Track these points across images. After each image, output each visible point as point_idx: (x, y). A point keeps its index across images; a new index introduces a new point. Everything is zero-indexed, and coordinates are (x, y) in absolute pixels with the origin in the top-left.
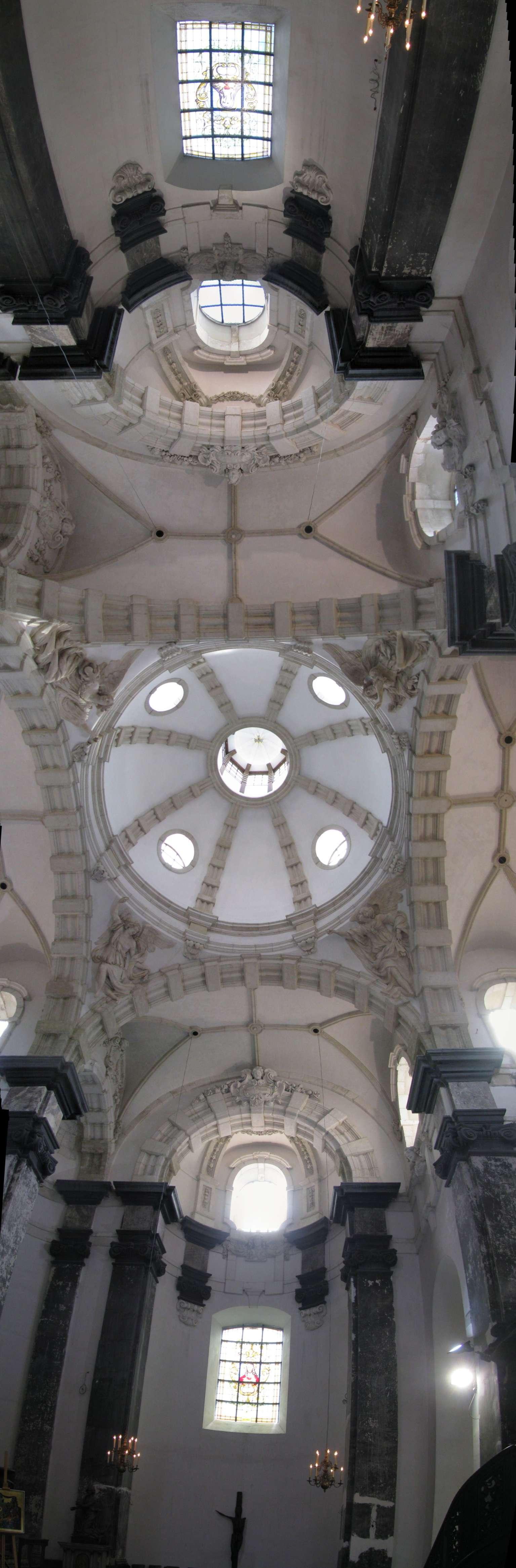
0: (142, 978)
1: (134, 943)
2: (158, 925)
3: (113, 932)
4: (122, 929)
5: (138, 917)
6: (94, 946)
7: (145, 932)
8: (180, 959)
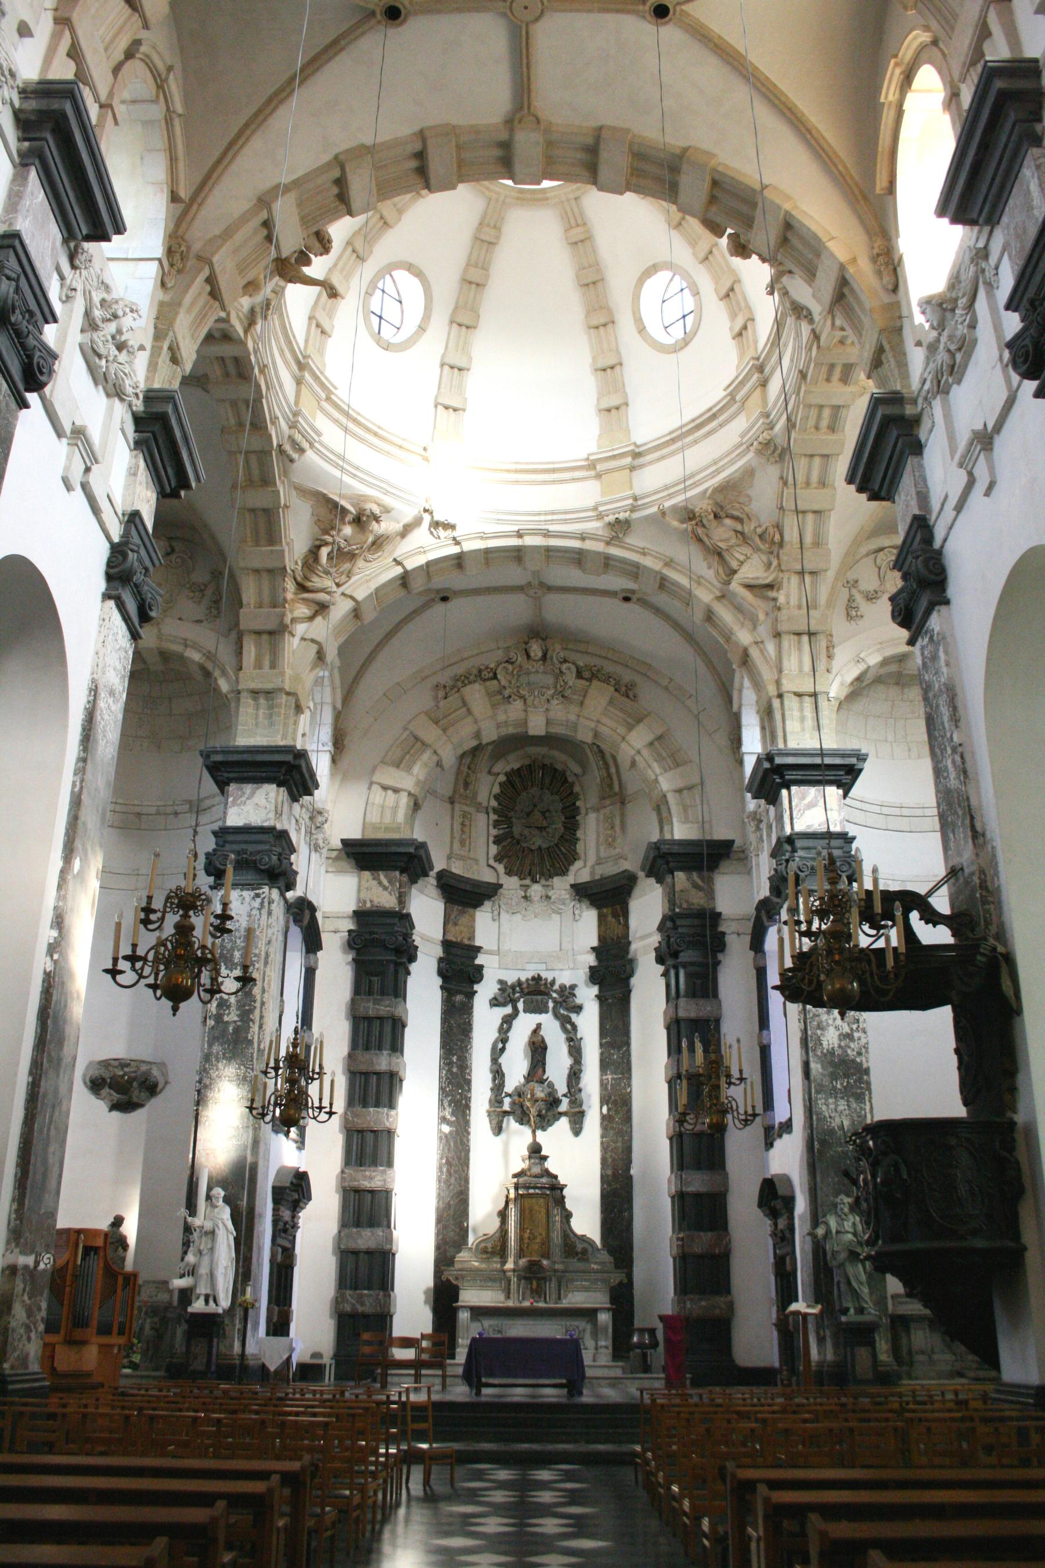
1: (728, 522)
2: (718, 472)
7: (719, 498)
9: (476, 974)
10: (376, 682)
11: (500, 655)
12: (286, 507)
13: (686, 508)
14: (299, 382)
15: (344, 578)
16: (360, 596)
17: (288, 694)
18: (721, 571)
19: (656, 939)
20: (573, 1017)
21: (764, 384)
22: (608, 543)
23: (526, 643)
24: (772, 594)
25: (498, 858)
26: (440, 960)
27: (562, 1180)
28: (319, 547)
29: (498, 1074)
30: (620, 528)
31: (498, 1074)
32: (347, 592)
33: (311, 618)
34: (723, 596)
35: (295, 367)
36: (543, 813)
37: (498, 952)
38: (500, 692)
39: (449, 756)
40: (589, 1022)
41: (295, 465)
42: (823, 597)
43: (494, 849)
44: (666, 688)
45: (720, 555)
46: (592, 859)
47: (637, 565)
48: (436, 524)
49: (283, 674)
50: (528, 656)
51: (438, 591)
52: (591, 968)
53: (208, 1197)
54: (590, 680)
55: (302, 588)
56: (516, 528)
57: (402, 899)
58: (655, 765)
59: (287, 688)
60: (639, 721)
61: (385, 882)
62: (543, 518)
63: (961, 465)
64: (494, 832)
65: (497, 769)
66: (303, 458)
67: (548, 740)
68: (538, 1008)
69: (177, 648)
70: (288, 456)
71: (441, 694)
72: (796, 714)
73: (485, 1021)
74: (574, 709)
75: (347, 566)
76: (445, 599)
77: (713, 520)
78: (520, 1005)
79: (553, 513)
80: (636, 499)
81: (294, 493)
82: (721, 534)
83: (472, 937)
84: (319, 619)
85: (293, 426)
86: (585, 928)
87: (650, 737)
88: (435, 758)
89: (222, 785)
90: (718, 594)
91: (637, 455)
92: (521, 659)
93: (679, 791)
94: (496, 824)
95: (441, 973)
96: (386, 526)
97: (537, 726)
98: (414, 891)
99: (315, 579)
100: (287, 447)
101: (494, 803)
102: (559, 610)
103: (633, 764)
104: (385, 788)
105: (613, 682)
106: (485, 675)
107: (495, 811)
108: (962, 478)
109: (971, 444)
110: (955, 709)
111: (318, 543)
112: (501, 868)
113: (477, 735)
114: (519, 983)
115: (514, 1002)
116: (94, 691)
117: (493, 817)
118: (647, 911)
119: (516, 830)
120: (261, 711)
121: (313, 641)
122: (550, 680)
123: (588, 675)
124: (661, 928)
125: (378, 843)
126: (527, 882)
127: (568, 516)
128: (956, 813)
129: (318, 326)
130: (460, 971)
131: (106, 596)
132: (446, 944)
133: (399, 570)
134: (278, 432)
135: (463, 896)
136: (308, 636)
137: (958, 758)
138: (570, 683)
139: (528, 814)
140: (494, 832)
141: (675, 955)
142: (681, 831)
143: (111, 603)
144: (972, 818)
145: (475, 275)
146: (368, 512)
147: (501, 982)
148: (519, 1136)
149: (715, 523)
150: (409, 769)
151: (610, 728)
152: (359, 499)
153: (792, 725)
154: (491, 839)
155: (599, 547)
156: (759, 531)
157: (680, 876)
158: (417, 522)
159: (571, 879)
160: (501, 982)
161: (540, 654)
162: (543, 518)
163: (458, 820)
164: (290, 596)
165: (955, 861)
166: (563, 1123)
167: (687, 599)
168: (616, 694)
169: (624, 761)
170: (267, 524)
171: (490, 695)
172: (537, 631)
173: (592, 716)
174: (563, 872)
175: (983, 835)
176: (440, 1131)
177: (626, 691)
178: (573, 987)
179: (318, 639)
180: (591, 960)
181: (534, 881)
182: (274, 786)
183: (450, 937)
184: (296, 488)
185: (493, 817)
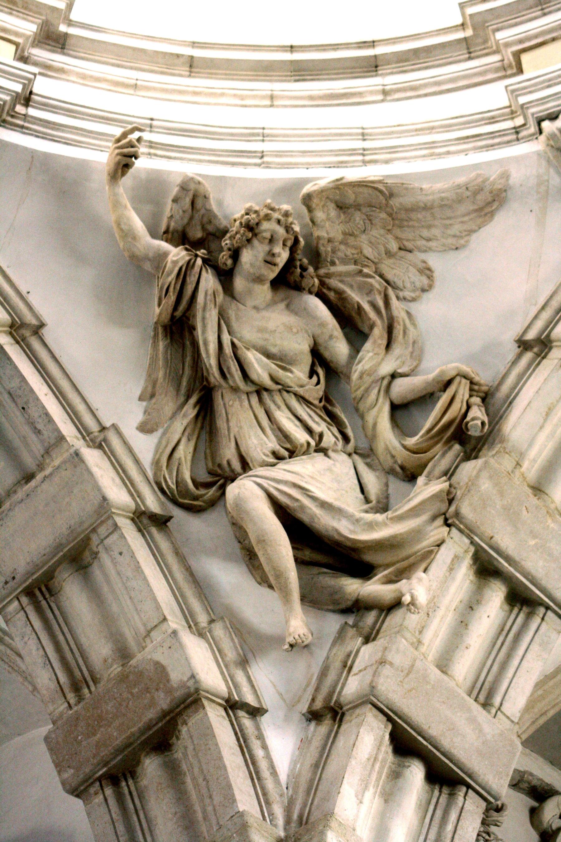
0: (461, 427)
2: (365, 157)
3: (178, 328)
4: (209, 282)
5: (238, 190)
6: (145, 447)
18: (185, 452)
80: (27, 99)
82: (272, 331)
149: (264, 292)
156: (402, 388)
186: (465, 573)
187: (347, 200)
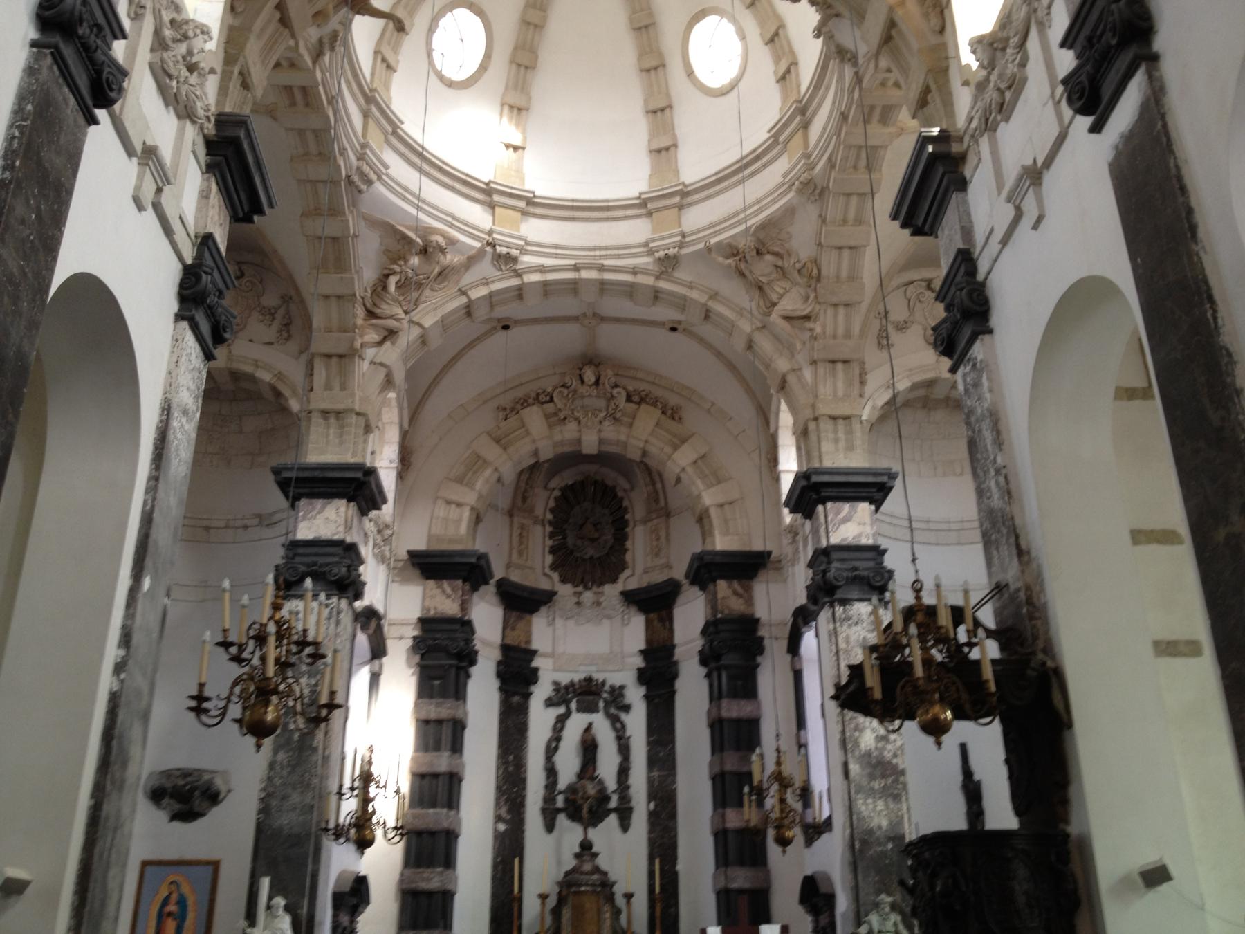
0: (812, 275)
1: (768, 257)
2: (761, 210)
3: (742, 275)
7: (761, 235)
8: (812, 211)
9: (532, 677)
10: (439, 405)
11: (556, 380)
12: (355, 236)
13: (730, 245)
14: (366, 115)
15: (412, 306)
16: (427, 323)
17: (358, 414)
18: (762, 303)
19: (699, 643)
20: (623, 716)
21: (806, 126)
22: (657, 278)
23: (581, 369)
24: (810, 325)
25: (554, 567)
26: (499, 663)
27: (612, 876)
28: (387, 276)
29: (551, 772)
30: (668, 264)
31: (551, 772)
32: (415, 319)
33: (380, 343)
34: (764, 327)
35: (362, 100)
36: (595, 525)
37: (552, 655)
38: (556, 414)
39: (509, 472)
40: (637, 722)
41: (365, 196)
42: (856, 330)
43: (549, 559)
44: (709, 411)
45: (760, 288)
46: (639, 568)
47: (684, 298)
48: (500, 256)
49: (353, 395)
50: (583, 382)
51: (499, 320)
52: (639, 670)
53: (269, 907)
54: (639, 403)
55: (371, 314)
56: (573, 262)
57: (464, 606)
58: (699, 482)
59: (357, 408)
60: (684, 441)
61: (449, 590)
62: (597, 253)
63: (1009, 200)
64: (549, 543)
65: (552, 484)
66: (371, 189)
67: (601, 458)
68: (589, 708)
69: (248, 369)
70: (357, 187)
71: (502, 415)
72: (831, 436)
73: (540, 719)
74: (624, 429)
75: (415, 295)
76: (506, 327)
77: (755, 255)
78: (573, 705)
79: (607, 248)
80: (683, 236)
81: (363, 223)
82: (762, 268)
83: (528, 642)
84: (388, 344)
85: (361, 157)
86: (633, 633)
87: (694, 456)
88: (496, 476)
89: (294, 501)
90: (759, 325)
91: (684, 194)
92: (575, 383)
93: (721, 506)
94: (552, 535)
95: (500, 675)
96: (451, 258)
97: (590, 445)
98: (476, 597)
99: (384, 306)
100: (356, 178)
101: (549, 516)
102: (610, 340)
103: (678, 480)
104: (449, 502)
105: (660, 405)
106: (543, 398)
107: (550, 523)
108: (1010, 212)
109: (1020, 179)
110: (998, 433)
111: (386, 272)
112: (556, 576)
113: (536, 453)
114: (572, 684)
115: (567, 702)
116: (167, 410)
117: (549, 529)
118: (690, 617)
119: (570, 541)
120: (332, 431)
121: (381, 364)
122: (602, 403)
123: (638, 399)
124: (704, 632)
125: (442, 554)
126: (580, 589)
127: (621, 252)
128: (999, 531)
129: (384, 60)
130: (517, 673)
131: (179, 317)
132: (506, 648)
133: (464, 300)
134: (348, 162)
135: (521, 602)
136: (378, 360)
137: (1002, 479)
138: (621, 407)
139: (581, 527)
140: (549, 543)
141: (718, 657)
142: (722, 543)
143: (185, 324)
144: (1017, 537)
145: (534, 16)
146: (434, 244)
147: (556, 683)
148: (570, 833)
150: (470, 485)
151: (658, 448)
152: (426, 232)
153: (827, 447)
154: (547, 549)
155: (650, 281)
156: (798, 266)
157: (722, 585)
158: (480, 254)
159: (619, 586)
160: (556, 683)
161: (593, 379)
162: (597, 253)
163: (516, 533)
164: (359, 322)
165: (999, 577)
166: (612, 820)
167: (731, 329)
168: (663, 417)
169: (670, 478)
170: (336, 252)
171: (547, 416)
172: (591, 360)
173: (641, 434)
174: (614, 580)
175: (1028, 553)
176: (496, 830)
177: (672, 413)
178: (622, 687)
179: (387, 362)
180: (639, 662)
181: (586, 588)
182: (344, 501)
183: (508, 641)
184: (365, 219)
185: (549, 529)
186: (830, 311)
187: (763, 226)
